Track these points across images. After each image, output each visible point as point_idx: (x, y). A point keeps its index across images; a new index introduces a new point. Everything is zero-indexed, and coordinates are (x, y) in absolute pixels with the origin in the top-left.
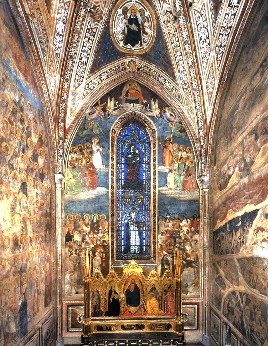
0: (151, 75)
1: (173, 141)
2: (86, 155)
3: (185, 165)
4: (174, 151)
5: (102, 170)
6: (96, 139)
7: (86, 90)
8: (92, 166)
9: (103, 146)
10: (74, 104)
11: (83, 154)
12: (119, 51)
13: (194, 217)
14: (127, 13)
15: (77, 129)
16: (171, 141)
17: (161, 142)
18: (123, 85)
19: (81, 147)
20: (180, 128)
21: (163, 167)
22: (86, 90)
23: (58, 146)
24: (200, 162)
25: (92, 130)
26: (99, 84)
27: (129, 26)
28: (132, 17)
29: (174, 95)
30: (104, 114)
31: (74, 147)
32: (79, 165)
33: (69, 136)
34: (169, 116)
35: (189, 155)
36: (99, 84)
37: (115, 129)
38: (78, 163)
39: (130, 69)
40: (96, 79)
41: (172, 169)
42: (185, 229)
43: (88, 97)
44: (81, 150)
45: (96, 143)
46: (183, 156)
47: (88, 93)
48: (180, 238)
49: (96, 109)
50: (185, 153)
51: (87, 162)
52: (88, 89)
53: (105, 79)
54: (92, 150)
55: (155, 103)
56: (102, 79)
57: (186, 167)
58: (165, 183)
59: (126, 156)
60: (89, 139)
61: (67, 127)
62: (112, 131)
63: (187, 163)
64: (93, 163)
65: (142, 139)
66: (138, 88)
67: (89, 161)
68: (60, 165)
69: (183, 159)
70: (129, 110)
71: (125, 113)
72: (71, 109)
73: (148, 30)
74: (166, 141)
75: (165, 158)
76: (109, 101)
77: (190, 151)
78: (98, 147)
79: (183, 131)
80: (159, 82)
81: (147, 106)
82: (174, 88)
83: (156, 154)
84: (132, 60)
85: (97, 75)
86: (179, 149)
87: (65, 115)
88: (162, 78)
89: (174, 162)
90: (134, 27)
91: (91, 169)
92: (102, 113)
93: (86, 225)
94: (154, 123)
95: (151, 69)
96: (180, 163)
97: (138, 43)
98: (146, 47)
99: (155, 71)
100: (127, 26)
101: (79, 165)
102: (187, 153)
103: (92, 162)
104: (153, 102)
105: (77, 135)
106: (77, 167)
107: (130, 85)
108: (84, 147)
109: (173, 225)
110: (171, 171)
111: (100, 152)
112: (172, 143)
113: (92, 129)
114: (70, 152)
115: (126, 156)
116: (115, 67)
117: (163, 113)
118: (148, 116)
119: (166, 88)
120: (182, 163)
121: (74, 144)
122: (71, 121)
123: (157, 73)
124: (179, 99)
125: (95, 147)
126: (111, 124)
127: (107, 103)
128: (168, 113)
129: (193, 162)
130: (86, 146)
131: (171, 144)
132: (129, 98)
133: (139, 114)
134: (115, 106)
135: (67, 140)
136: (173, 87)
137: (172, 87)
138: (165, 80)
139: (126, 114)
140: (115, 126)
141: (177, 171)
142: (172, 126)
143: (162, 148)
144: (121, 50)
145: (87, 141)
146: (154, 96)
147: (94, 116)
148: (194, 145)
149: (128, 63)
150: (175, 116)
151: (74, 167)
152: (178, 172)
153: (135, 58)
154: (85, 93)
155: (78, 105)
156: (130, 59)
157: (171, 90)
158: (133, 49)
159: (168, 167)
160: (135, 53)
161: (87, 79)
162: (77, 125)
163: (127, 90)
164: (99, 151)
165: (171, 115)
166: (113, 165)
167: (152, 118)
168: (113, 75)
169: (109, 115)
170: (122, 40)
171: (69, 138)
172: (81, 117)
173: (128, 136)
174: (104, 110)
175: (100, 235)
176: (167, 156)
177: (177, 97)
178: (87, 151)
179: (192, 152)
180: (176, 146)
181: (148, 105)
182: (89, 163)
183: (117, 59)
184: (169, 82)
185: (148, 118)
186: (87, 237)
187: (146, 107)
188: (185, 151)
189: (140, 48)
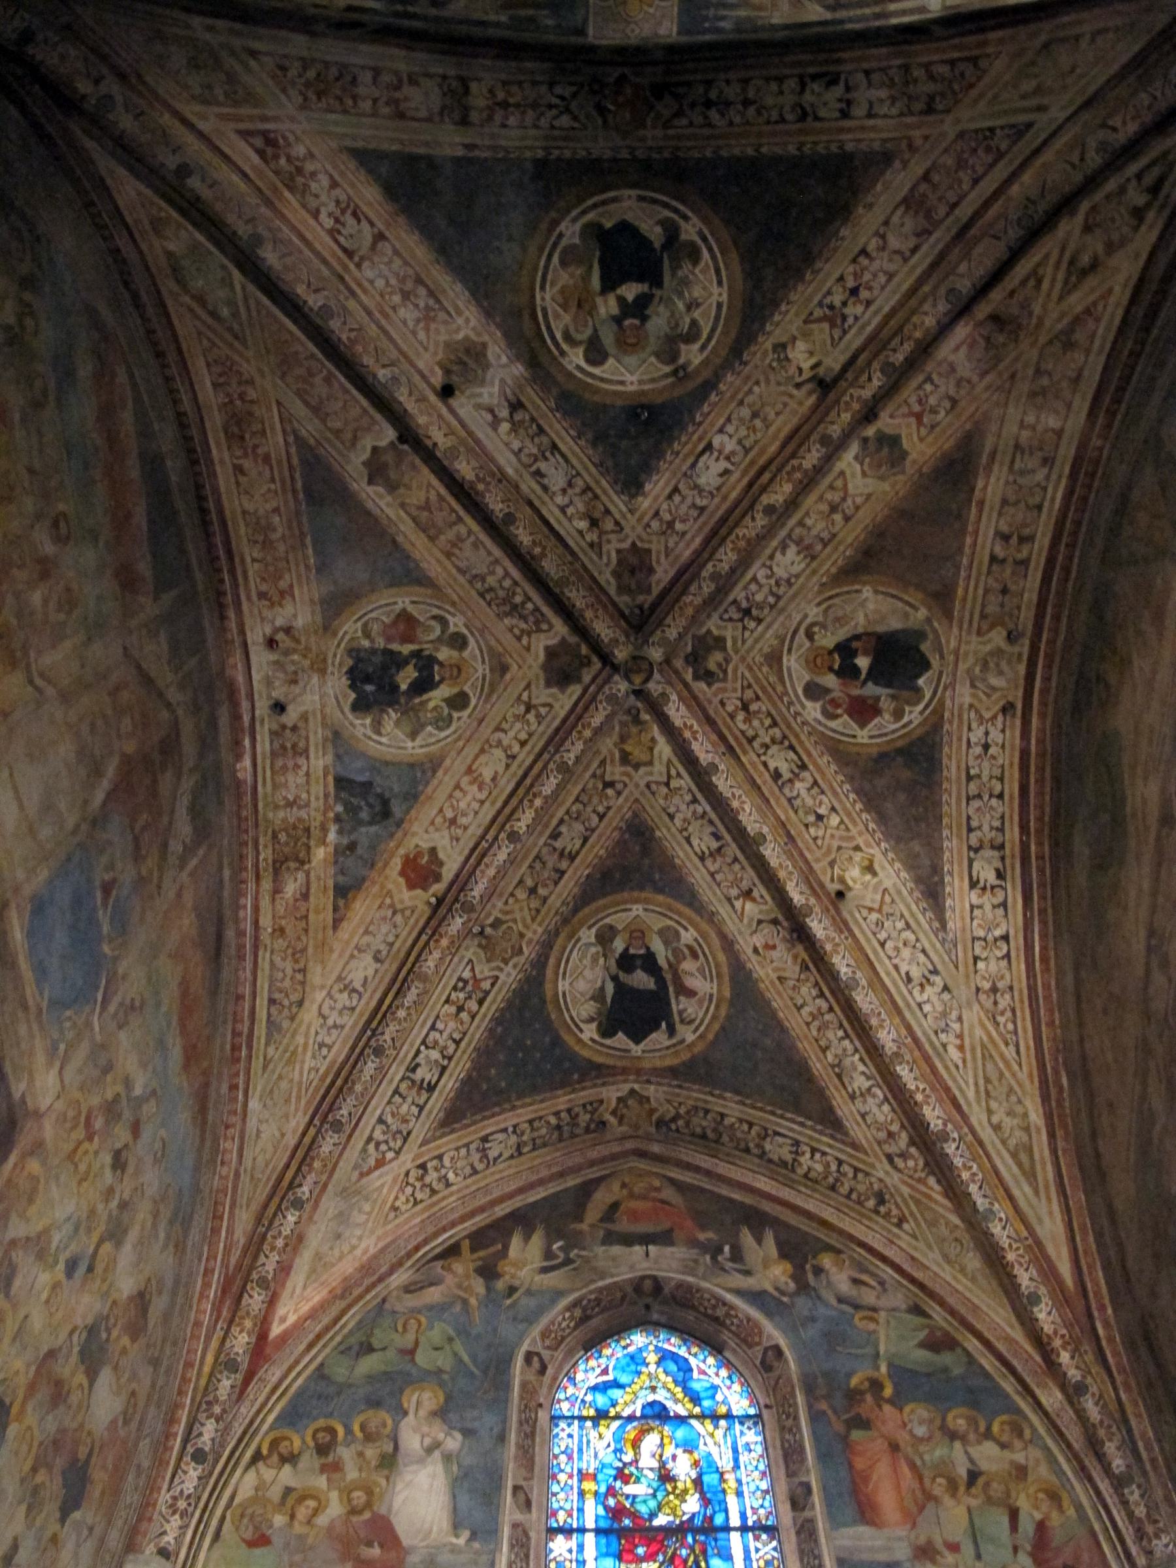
0: (725, 1138)
1: (897, 1392)
2: (352, 1474)
3: (1014, 1514)
4: (921, 1440)
5: (444, 1558)
6: (427, 1395)
7: (409, 1190)
9: (469, 1425)
10: (338, 1236)
11: (333, 1468)
12: (576, 1054)
14: (612, 940)
15: (327, 1350)
16: (888, 1392)
17: (828, 1397)
18: (586, 1190)
19: (332, 1431)
20: (922, 1335)
21: (863, 1529)
22: (409, 1190)
23: (205, 1402)
24: (1104, 1486)
25: (412, 1352)
26: (475, 1172)
27: (622, 976)
28: (632, 951)
29: (854, 1196)
30: (489, 1289)
31: (287, 1432)
32: (298, 1528)
33: (272, 1373)
34: (845, 1287)
35: (1020, 1457)
36: (475, 1172)
37: (546, 1354)
38: (292, 1516)
39: (624, 1128)
40: (463, 1151)
41: (930, 1542)
43: (411, 1221)
45: (422, 1413)
46: (984, 1466)
47: (416, 1203)
49: (448, 1269)
50: (990, 1448)
51: (354, 1511)
52: (418, 1185)
53: (506, 1155)
54: (396, 1448)
55: (759, 1241)
56: (492, 1154)
57: (1027, 1526)
59: (611, 1491)
61: (276, 1330)
62: (529, 1357)
63: (1023, 1503)
64: (395, 1521)
65: (706, 1403)
66: (669, 1193)
67: (368, 1505)
68: (182, 1504)
69: (987, 1485)
70: (624, 1269)
71: (600, 1284)
72: (318, 1256)
73: (694, 982)
74: (854, 1396)
75: (866, 1479)
76: (516, 1242)
77: (1020, 1435)
78: (438, 1431)
80: (770, 1161)
81: (720, 1250)
82: (845, 1168)
83: (803, 1460)
84: (632, 1092)
85: (473, 1134)
86: (943, 1428)
87: (284, 1269)
88: (780, 1140)
89: (936, 1500)
90: (641, 980)
91: (376, 1551)
92: (479, 1286)
94: (769, 1315)
95: (722, 1116)
96: (974, 1502)
97: (657, 1027)
98: (690, 1038)
99: (741, 1121)
100: (615, 979)
101: (298, 1528)
102: (1003, 1446)
103: (383, 1511)
104: (747, 1238)
105: (320, 1373)
106: (277, 1540)
107: (624, 1185)
108: (349, 1431)
111: (447, 1458)
112: (897, 1402)
113: (410, 1346)
114: (257, 1457)
115: (611, 1491)
116: (557, 1114)
117: (810, 1277)
118: (729, 1290)
119: (806, 1176)
120: (989, 1501)
121: (292, 1416)
122: (305, 1308)
123: (751, 1125)
124: (882, 1209)
126: (521, 1327)
127: (506, 1247)
128: (840, 1279)
129: (1065, 1496)
130: (363, 1428)
131: (887, 1408)
132: (623, 1225)
133: (680, 1285)
134: (548, 1254)
135: (257, 1393)
136: (840, 1162)
137: (834, 1167)
138: (797, 1143)
139: (607, 1288)
140: (544, 1335)
141: (968, 1549)
142: (872, 1326)
143: (839, 1427)
144: (585, 1053)
145: (375, 1403)
146: (757, 1220)
147: (433, 1295)
148: (1038, 1404)
149: (614, 1103)
150: (882, 1283)
151: (261, 1540)
152: (978, 1557)
153: (648, 1082)
154: (403, 1198)
155: (354, 1241)
156: (626, 1087)
157: (831, 1180)
158: (637, 1050)
159: (902, 1532)
160: (647, 1065)
161: (425, 1142)
162: (327, 1329)
163: (610, 1199)
164: (437, 1454)
165: (855, 1281)
166: (526, 1534)
167: (757, 1297)
168: (545, 1145)
169: (512, 1290)
170: (591, 1020)
171: (275, 1379)
172: (360, 1297)
173: (621, 1386)
174: (488, 1272)
176: (883, 1469)
177: (871, 1203)
178: (361, 1454)
179: (1035, 1440)
180: (925, 1414)
181: (727, 1248)
182: (367, 1515)
183: (563, 1085)
184: (814, 1151)
185: (729, 1297)
187: (714, 1258)
188: (988, 1435)
189: (668, 1043)
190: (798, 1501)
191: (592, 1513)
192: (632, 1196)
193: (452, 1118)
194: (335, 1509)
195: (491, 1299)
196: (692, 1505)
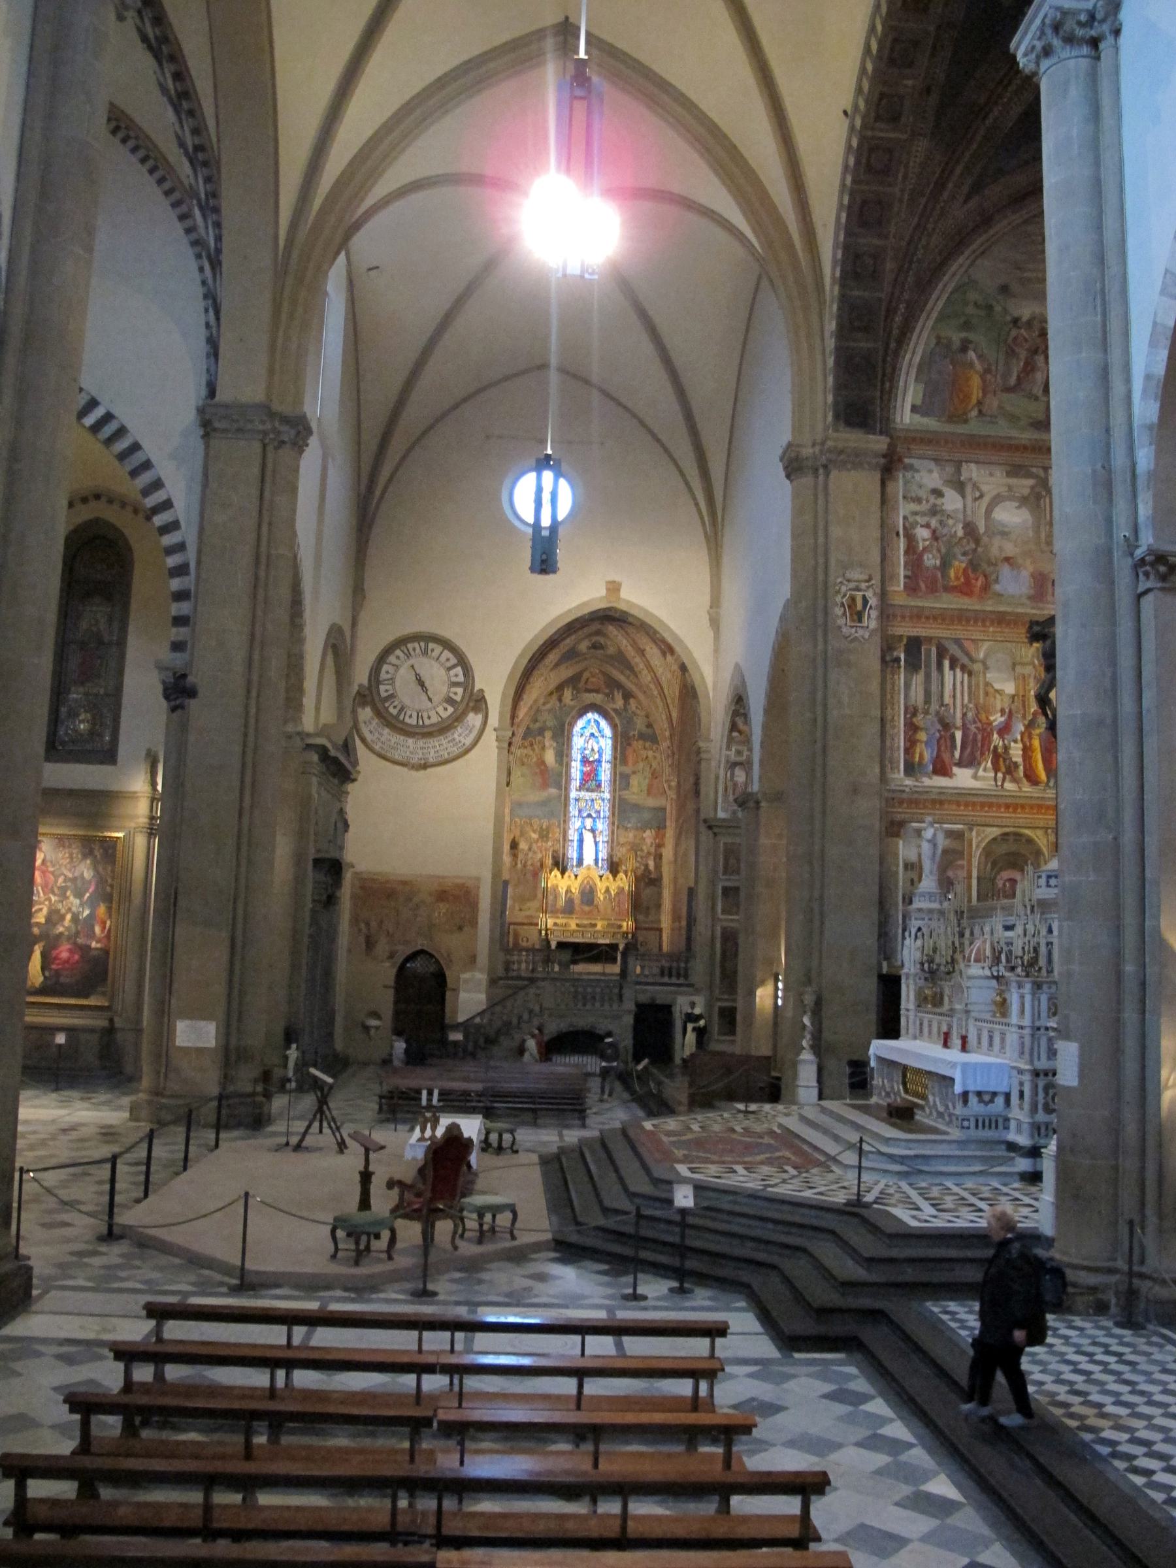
8: (543, 763)
11: (533, 750)
13: (659, 828)
42: (649, 841)
44: (532, 745)
48: (642, 850)
58: (627, 786)
60: (541, 731)
79: (649, 726)
93: (534, 832)
105: (528, 728)
109: (635, 836)
110: (634, 773)
121: (524, 738)
125: (548, 742)
132: (589, 686)
146: (619, 686)
147: (548, 706)
151: (523, 764)
167: (615, 710)
174: (560, 700)
175: (550, 844)
186: (535, 847)
190: (615, 758)
191: (579, 757)
192: (593, 676)
193: (552, 670)
194: (535, 760)
195: (561, 708)
196: (597, 756)
